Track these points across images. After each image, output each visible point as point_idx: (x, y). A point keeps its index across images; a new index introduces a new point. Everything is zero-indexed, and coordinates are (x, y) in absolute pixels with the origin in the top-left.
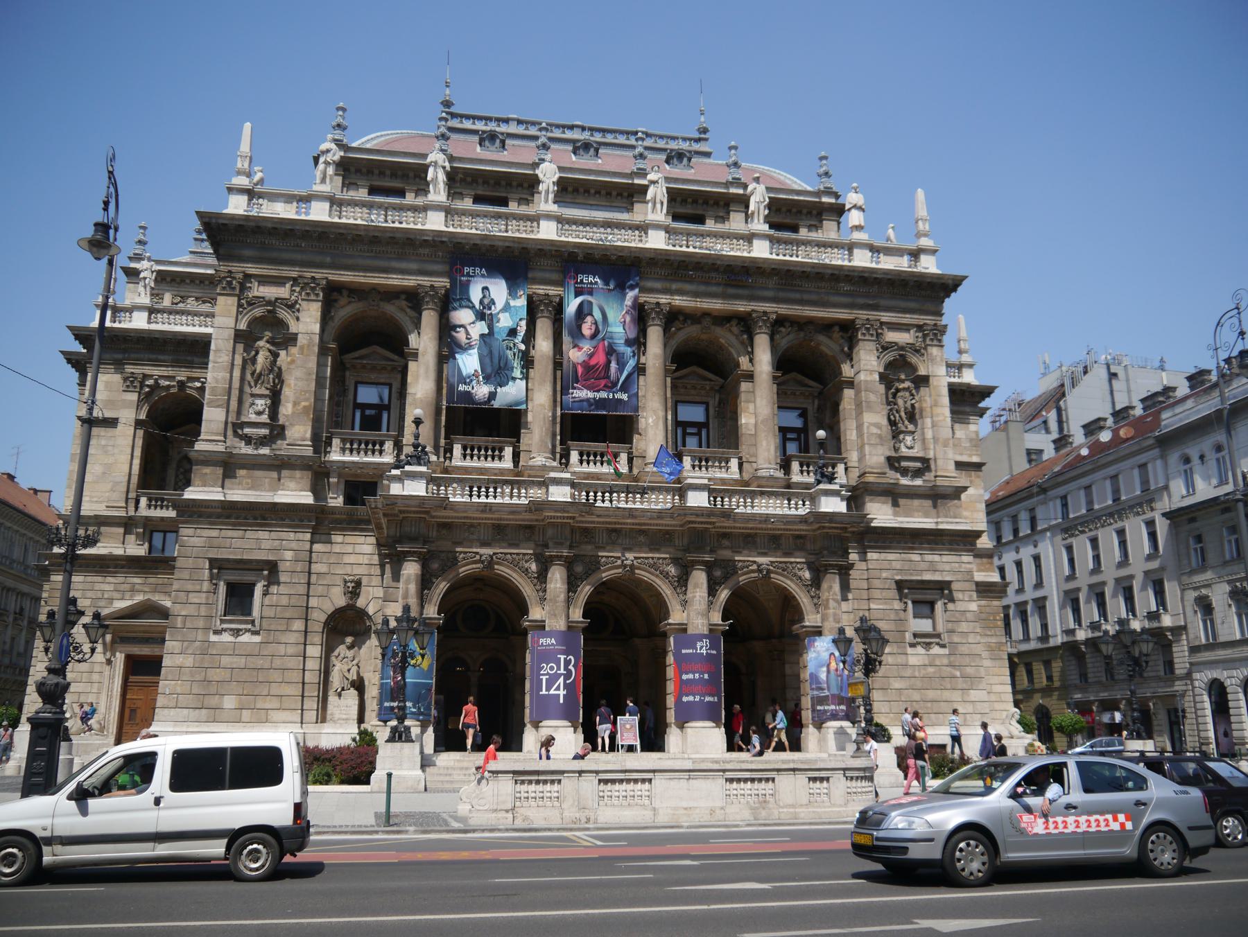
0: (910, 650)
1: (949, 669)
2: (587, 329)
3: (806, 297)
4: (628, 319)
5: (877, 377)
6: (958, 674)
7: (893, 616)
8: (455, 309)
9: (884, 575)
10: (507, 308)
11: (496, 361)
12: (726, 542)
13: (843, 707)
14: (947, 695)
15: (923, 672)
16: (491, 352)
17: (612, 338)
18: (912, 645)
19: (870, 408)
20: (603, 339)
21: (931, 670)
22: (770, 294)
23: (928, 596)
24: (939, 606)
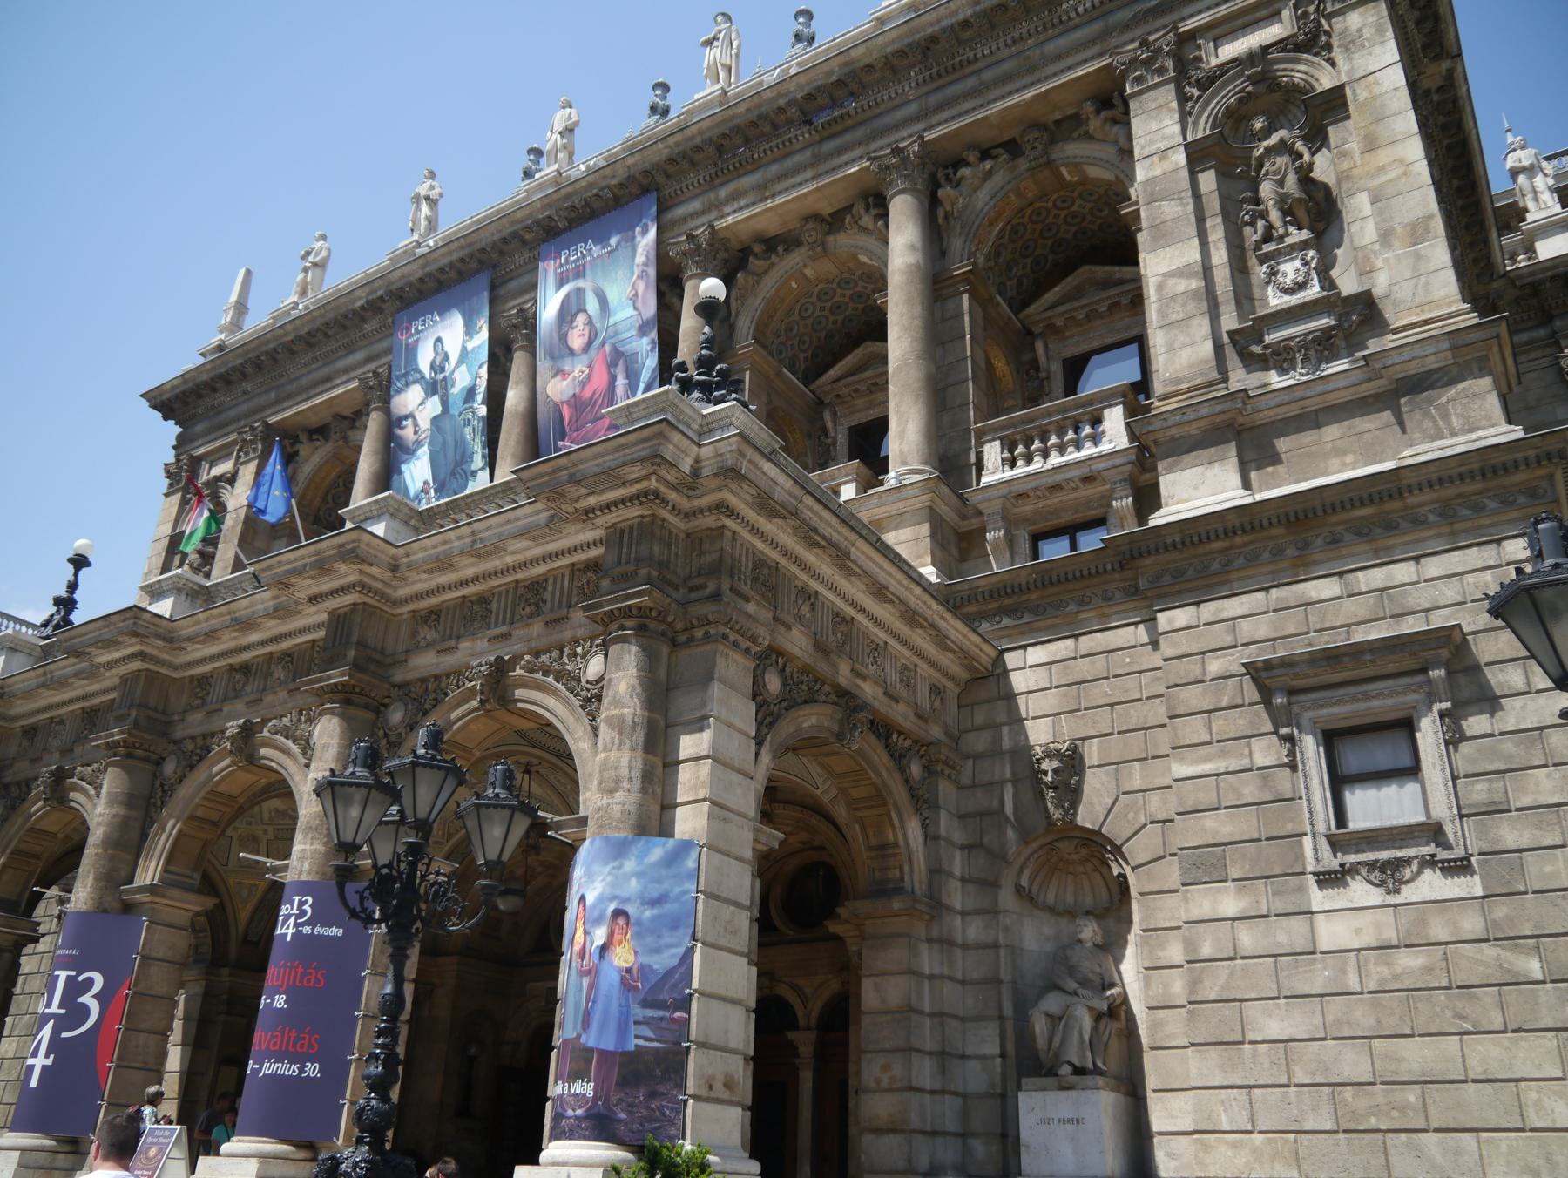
0: (1318, 898)
1: (1490, 952)
2: (576, 340)
3: (987, 76)
4: (641, 286)
5: (1180, 158)
6: (1534, 968)
7: (1250, 790)
8: (399, 391)
9: (1215, 666)
10: (464, 355)
11: (451, 453)
12: (428, 634)
13: (586, 1088)
14: (1486, 1054)
15: (1377, 973)
16: (444, 443)
17: (616, 334)
18: (1331, 879)
19: (1164, 237)
20: (603, 344)
21: (1410, 961)
22: (912, 109)
23: (1382, 702)
24: (1429, 733)
